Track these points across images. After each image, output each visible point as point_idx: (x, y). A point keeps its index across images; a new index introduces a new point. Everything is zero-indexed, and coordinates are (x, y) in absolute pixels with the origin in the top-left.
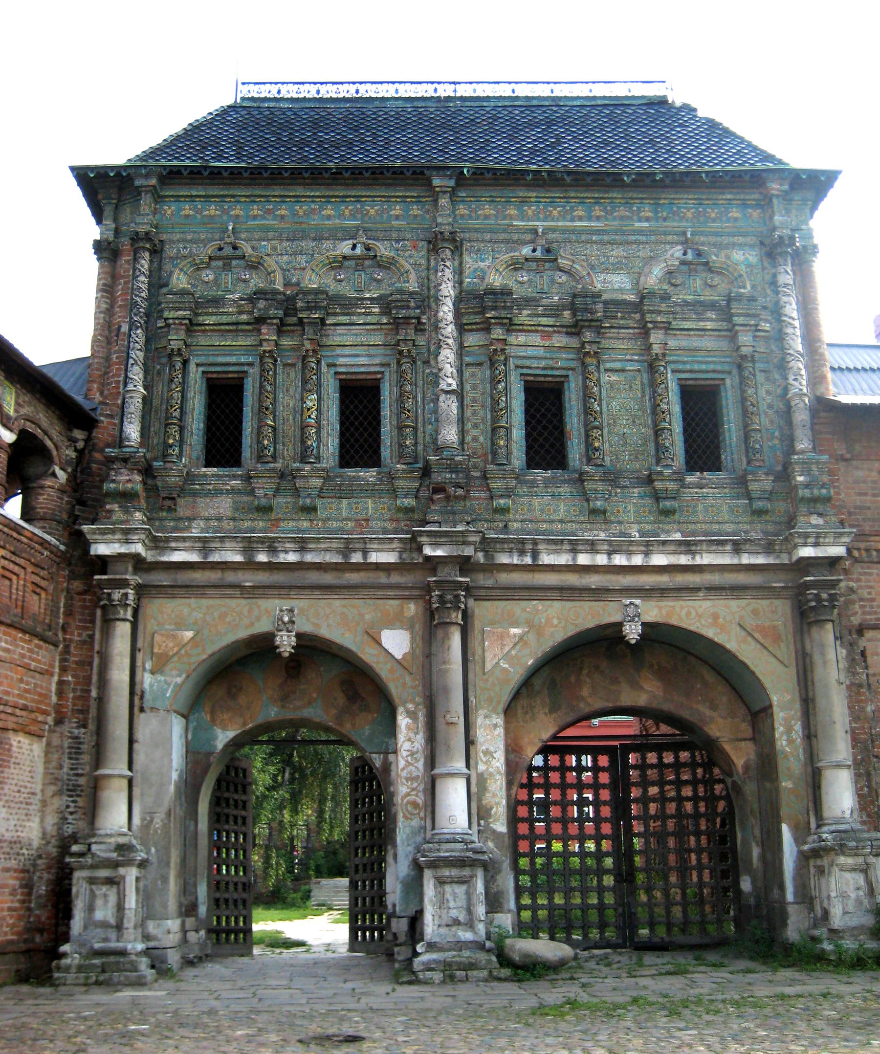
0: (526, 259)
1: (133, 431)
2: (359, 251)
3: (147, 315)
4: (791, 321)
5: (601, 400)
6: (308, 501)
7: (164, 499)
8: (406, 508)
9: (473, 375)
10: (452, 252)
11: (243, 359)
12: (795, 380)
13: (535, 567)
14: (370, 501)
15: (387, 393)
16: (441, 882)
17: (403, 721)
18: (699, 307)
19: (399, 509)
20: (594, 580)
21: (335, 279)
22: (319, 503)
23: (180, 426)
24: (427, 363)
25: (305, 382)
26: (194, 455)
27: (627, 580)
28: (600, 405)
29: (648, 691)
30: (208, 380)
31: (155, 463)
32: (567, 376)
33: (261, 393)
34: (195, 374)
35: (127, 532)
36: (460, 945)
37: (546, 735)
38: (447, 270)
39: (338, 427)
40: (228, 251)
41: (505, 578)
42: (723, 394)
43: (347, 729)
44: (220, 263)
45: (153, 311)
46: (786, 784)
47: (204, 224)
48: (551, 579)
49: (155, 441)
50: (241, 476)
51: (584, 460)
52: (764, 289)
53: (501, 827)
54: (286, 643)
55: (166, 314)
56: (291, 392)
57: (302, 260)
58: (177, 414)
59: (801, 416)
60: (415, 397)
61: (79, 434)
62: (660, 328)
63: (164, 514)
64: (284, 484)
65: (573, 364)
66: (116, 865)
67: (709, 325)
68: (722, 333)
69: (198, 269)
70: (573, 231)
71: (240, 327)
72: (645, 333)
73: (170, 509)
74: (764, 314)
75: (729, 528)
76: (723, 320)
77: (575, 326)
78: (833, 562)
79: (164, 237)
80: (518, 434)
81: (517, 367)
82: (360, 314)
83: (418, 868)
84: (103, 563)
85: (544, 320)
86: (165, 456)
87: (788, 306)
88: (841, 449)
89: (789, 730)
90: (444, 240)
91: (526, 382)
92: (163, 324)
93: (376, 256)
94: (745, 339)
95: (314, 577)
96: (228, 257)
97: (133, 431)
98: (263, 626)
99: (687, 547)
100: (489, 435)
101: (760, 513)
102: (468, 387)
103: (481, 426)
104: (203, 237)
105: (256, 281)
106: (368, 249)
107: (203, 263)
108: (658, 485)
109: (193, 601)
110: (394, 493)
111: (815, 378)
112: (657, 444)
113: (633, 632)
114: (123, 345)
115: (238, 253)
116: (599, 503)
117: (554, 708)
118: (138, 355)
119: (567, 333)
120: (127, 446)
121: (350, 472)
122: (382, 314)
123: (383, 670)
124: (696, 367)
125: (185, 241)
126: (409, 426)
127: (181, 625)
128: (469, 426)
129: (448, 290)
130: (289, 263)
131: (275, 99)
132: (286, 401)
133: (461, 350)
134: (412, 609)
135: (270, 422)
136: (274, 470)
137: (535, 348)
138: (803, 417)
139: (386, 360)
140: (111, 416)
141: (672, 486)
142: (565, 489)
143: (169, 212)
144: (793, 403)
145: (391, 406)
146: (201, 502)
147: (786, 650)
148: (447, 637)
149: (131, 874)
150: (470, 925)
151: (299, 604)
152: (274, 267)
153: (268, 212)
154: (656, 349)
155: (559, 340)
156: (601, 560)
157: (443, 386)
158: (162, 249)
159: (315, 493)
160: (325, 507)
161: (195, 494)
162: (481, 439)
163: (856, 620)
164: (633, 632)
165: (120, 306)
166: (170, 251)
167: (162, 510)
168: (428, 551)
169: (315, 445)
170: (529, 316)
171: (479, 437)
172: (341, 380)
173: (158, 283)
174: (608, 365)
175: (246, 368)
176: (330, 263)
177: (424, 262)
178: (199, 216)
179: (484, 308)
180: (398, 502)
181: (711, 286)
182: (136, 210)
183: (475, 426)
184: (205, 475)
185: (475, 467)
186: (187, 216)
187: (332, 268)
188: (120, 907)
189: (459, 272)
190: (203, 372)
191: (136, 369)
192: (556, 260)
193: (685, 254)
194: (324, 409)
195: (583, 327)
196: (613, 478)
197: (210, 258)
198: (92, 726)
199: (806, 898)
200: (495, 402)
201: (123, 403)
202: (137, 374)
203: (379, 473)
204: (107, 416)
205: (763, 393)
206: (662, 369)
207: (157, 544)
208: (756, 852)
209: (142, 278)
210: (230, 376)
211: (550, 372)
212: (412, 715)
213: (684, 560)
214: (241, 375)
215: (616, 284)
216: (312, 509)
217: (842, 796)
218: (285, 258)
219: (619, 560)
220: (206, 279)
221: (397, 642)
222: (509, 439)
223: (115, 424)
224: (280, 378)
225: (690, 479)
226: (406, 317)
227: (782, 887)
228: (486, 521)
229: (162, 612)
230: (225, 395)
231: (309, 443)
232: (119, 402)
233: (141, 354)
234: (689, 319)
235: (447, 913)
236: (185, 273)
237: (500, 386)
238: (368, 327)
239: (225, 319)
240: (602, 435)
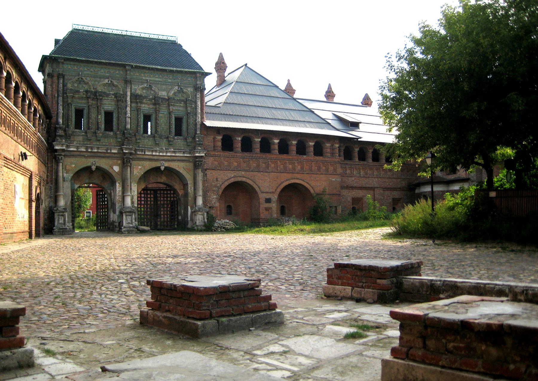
1: (61, 121)
13: (145, 155)
16: (126, 216)
17: (117, 184)
18: (180, 101)
20: (155, 158)
25: (98, 112)
27: (162, 158)
29: (163, 179)
34: (73, 108)
35: (62, 144)
36: (130, 227)
37: (143, 187)
40: (80, 79)
41: (138, 156)
43: (103, 185)
45: (64, 92)
46: (190, 199)
48: (147, 157)
53: (136, 205)
54: (94, 168)
57: (97, 83)
59: (198, 126)
61: (48, 120)
66: (64, 212)
70: (155, 81)
72: (169, 106)
74: (193, 103)
75: (182, 148)
78: (202, 156)
83: (121, 213)
84: (56, 150)
86: (68, 127)
88: (205, 133)
89: (191, 188)
94: (189, 109)
95: (99, 154)
96: (80, 81)
97: (61, 121)
98: (89, 164)
99: (174, 152)
101: (188, 146)
105: (86, 87)
106: (111, 81)
109: (74, 159)
110: (117, 138)
113: (162, 168)
117: (145, 182)
118: (61, 103)
121: (107, 132)
123: (114, 174)
127: (72, 163)
129: (129, 94)
131: (82, 30)
132: (93, 115)
134: (119, 162)
137: (146, 107)
141: (172, 139)
146: (76, 137)
147: (192, 173)
148: (127, 168)
149: (66, 214)
150: (132, 223)
151: (96, 160)
153: (88, 70)
154: (171, 110)
155: (151, 106)
156: (158, 154)
157: (127, 116)
160: (103, 140)
161: (74, 135)
163: (205, 168)
164: (162, 168)
166: (66, 77)
168: (124, 151)
171: (134, 127)
179: (136, 98)
188: (64, 220)
189: (131, 89)
198: (54, 184)
199: (192, 220)
202: (61, 108)
205: (191, 121)
207: (68, 146)
208: (182, 211)
212: (119, 183)
213: (173, 155)
215: (163, 94)
216: (99, 140)
217: (200, 201)
219: (161, 154)
221: (116, 169)
225: (176, 138)
226: (119, 99)
227: (188, 218)
229: (68, 161)
230: (79, 113)
235: (128, 221)
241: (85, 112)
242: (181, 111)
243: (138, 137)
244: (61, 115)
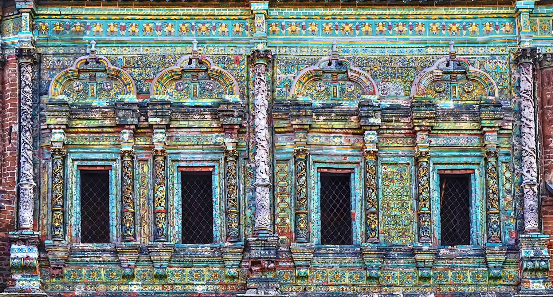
0: (324, 72)
2: (194, 65)
3: (33, 119)
4: (528, 122)
5: (378, 189)
6: (160, 270)
7: (53, 268)
8: (232, 276)
9: (282, 169)
10: (266, 66)
11: (108, 156)
12: (528, 172)
14: (205, 270)
15: (217, 184)
19: (227, 277)
21: (176, 89)
22: (168, 271)
23: (63, 212)
24: (247, 159)
25: (155, 176)
26: (74, 233)
28: (377, 195)
30: (81, 171)
31: (46, 242)
32: (354, 169)
33: (122, 185)
34: (72, 170)
38: (262, 83)
39: (181, 210)
40: (93, 64)
42: (473, 181)
44: (87, 75)
47: (72, 39)
49: (45, 222)
50: (110, 251)
51: (364, 237)
52: (510, 92)
55: (49, 121)
56: (146, 182)
58: (60, 202)
60: (238, 188)
62: (425, 131)
63: (54, 280)
64: (143, 257)
65: (357, 159)
67: (465, 126)
68: (473, 132)
69: (70, 80)
71: (105, 130)
73: (58, 277)
76: (475, 121)
77: (360, 128)
79: (42, 50)
80: (316, 217)
81: (315, 162)
82: (196, 120)
85: (336, 124)
87: (526, 108)
90: (260, 58)
91: (321, 173)
92: (46, 127)
93: (207, 70)
97: (27, 215)
100: (293, 218)
102: (277, 179)
103: (288, 210)
104: (72, 51)
107: (73, 76)
108: (418, 257)
111: (546, 167)
112: (419, 225)
114: (15, 144)
115: (101, 67)
116: (374, 272)
119: (354, 134)
120: (24, 229)
121: (190, 247)
122: (212, 119)
124: (453, 160)
125: (57, 54)
126: (234, 213)
128: (279, 210)
130: (140, 75)
132: (143, 189)
133: (273, 149)
135: (131, 209)
136: (135, 247)
138: (532, 202)
139: (217, 157)
140: (10, 202)
141: (429, 258)
142: (349, 261)
143: (44, 28)
144: (525, 191)
145: (220, 194)
152: (129, 80)
153: (124, 28)
157: (259, 181)
158: (40, 62)
159: (165, 264)
162: (288, 221)
165: (11, 110)
166: (47, 63)
167: (52, 276)
169: (164, 227)
170: (324, 121)
173: (39, 91)
174: (385, 160)
175: (110, 163)
176: (172, 76)
177: (245, 74)
178: (68, 32)
180: (227, 272)
181: (467, 92)
182: (18, 28)
183: (283, 210)
184: (83, 250)
185: (283, 243)
186: (58, 32)
187: (174, 80)
189: (272, 82)
190: (78, 166)
191: (27, 165)
192: (347, 72)
193: (448, 65)
194: (170, 197)
195: (365, 130)
196: (385, 253)
197: (79, 72)
200: (298, 192)
201: (19, 189)
202: (28, 169)
203: (212, 248)
204: (5, 202)
206: (425, 164)
209: (27, 89)
210: (98, 168)
211: (340, 166)
214: (107, 168)
218: (137, 70)
220: (77, 89)
222: (308, 221)
223: (13, 208)
224: (136, 172)
228: (290, 284)
230: (94, 182)
231: (160, 225)
232: (15, 190)
233: (30, 153)
234: (448, 121)
236: (61, 84)
237: (301, 180)
238: (202, 130)
239: (92, 123)
240: (378, 219)
241: (114, 177)
242: (464, 149)
243: (299, 258)
244: (28, 194)
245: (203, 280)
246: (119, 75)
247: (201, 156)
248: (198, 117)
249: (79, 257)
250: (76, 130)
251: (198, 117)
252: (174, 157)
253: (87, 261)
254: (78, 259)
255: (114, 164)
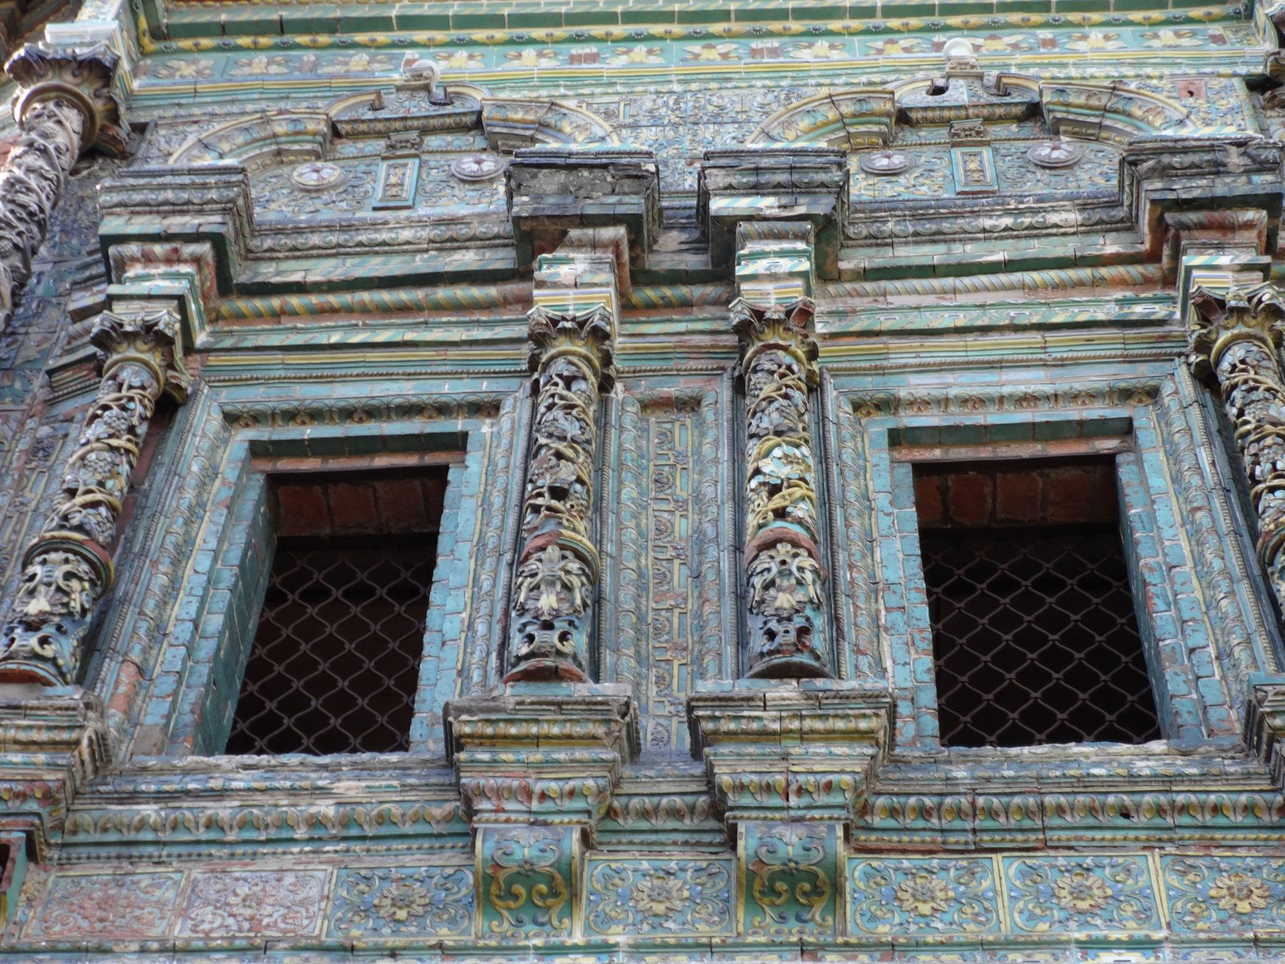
11: (449, 389)
14: (1153, 861)
139: (1142, 374)
161: (127, 848)
172: (920, 469)
175: (458, 424)
245: (1144, 915)
246: (551, 118)
247: (1041, 374)
248: (1008, 221)
249: (159, 797)
250: (276, 302)
251: (1008, 221)
252: (869, 385)
253: (211, 824)
254: (149, 811)
255: (483, 428)
